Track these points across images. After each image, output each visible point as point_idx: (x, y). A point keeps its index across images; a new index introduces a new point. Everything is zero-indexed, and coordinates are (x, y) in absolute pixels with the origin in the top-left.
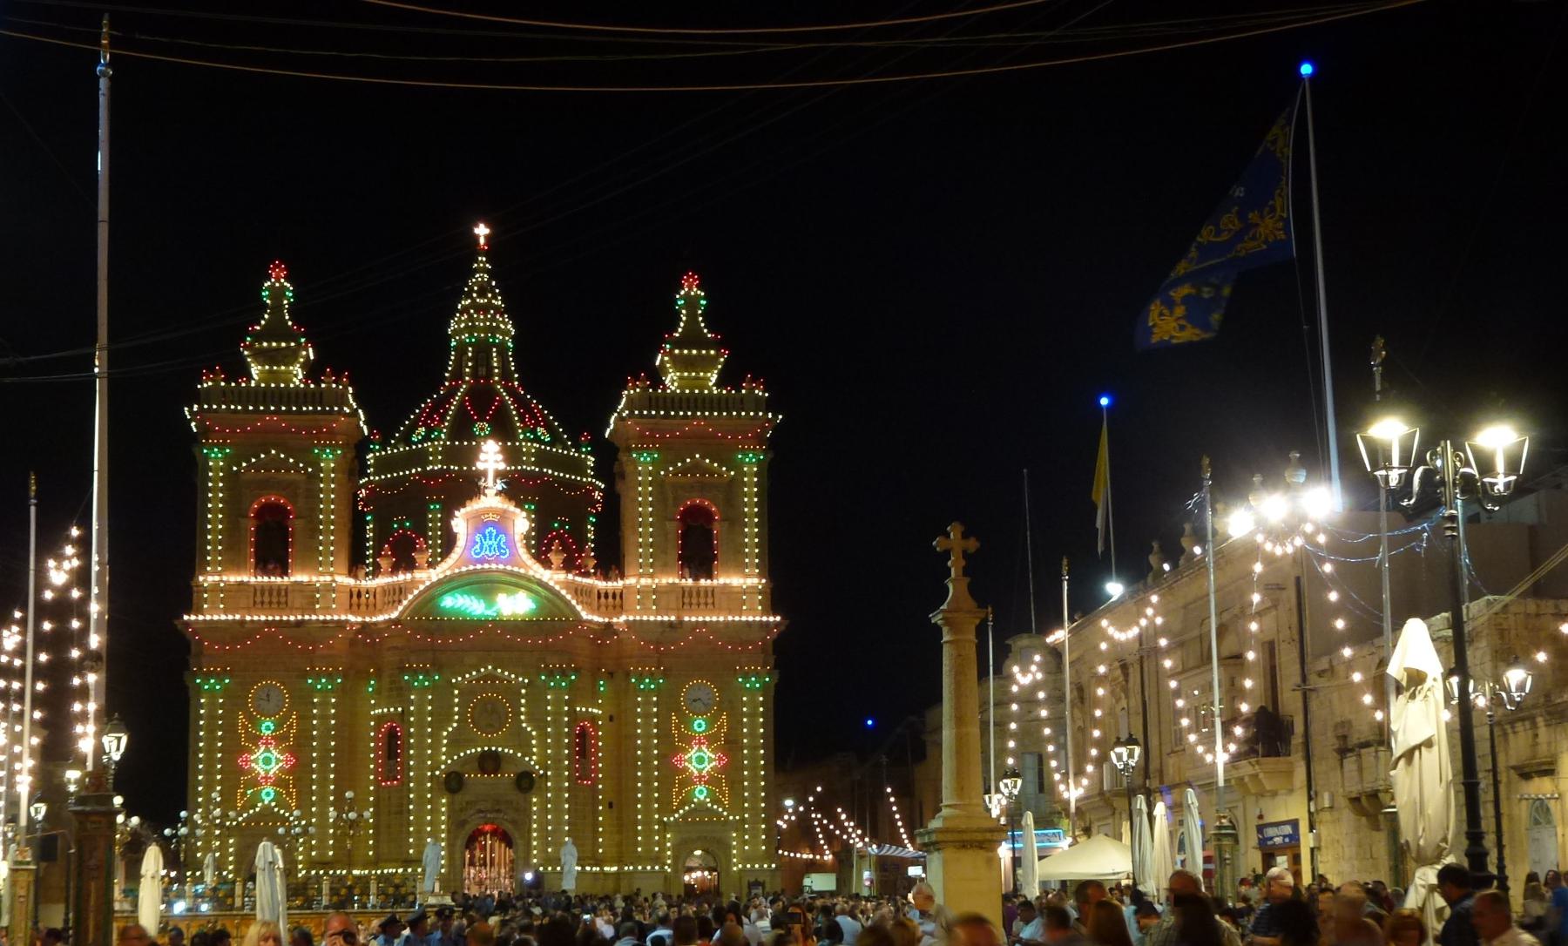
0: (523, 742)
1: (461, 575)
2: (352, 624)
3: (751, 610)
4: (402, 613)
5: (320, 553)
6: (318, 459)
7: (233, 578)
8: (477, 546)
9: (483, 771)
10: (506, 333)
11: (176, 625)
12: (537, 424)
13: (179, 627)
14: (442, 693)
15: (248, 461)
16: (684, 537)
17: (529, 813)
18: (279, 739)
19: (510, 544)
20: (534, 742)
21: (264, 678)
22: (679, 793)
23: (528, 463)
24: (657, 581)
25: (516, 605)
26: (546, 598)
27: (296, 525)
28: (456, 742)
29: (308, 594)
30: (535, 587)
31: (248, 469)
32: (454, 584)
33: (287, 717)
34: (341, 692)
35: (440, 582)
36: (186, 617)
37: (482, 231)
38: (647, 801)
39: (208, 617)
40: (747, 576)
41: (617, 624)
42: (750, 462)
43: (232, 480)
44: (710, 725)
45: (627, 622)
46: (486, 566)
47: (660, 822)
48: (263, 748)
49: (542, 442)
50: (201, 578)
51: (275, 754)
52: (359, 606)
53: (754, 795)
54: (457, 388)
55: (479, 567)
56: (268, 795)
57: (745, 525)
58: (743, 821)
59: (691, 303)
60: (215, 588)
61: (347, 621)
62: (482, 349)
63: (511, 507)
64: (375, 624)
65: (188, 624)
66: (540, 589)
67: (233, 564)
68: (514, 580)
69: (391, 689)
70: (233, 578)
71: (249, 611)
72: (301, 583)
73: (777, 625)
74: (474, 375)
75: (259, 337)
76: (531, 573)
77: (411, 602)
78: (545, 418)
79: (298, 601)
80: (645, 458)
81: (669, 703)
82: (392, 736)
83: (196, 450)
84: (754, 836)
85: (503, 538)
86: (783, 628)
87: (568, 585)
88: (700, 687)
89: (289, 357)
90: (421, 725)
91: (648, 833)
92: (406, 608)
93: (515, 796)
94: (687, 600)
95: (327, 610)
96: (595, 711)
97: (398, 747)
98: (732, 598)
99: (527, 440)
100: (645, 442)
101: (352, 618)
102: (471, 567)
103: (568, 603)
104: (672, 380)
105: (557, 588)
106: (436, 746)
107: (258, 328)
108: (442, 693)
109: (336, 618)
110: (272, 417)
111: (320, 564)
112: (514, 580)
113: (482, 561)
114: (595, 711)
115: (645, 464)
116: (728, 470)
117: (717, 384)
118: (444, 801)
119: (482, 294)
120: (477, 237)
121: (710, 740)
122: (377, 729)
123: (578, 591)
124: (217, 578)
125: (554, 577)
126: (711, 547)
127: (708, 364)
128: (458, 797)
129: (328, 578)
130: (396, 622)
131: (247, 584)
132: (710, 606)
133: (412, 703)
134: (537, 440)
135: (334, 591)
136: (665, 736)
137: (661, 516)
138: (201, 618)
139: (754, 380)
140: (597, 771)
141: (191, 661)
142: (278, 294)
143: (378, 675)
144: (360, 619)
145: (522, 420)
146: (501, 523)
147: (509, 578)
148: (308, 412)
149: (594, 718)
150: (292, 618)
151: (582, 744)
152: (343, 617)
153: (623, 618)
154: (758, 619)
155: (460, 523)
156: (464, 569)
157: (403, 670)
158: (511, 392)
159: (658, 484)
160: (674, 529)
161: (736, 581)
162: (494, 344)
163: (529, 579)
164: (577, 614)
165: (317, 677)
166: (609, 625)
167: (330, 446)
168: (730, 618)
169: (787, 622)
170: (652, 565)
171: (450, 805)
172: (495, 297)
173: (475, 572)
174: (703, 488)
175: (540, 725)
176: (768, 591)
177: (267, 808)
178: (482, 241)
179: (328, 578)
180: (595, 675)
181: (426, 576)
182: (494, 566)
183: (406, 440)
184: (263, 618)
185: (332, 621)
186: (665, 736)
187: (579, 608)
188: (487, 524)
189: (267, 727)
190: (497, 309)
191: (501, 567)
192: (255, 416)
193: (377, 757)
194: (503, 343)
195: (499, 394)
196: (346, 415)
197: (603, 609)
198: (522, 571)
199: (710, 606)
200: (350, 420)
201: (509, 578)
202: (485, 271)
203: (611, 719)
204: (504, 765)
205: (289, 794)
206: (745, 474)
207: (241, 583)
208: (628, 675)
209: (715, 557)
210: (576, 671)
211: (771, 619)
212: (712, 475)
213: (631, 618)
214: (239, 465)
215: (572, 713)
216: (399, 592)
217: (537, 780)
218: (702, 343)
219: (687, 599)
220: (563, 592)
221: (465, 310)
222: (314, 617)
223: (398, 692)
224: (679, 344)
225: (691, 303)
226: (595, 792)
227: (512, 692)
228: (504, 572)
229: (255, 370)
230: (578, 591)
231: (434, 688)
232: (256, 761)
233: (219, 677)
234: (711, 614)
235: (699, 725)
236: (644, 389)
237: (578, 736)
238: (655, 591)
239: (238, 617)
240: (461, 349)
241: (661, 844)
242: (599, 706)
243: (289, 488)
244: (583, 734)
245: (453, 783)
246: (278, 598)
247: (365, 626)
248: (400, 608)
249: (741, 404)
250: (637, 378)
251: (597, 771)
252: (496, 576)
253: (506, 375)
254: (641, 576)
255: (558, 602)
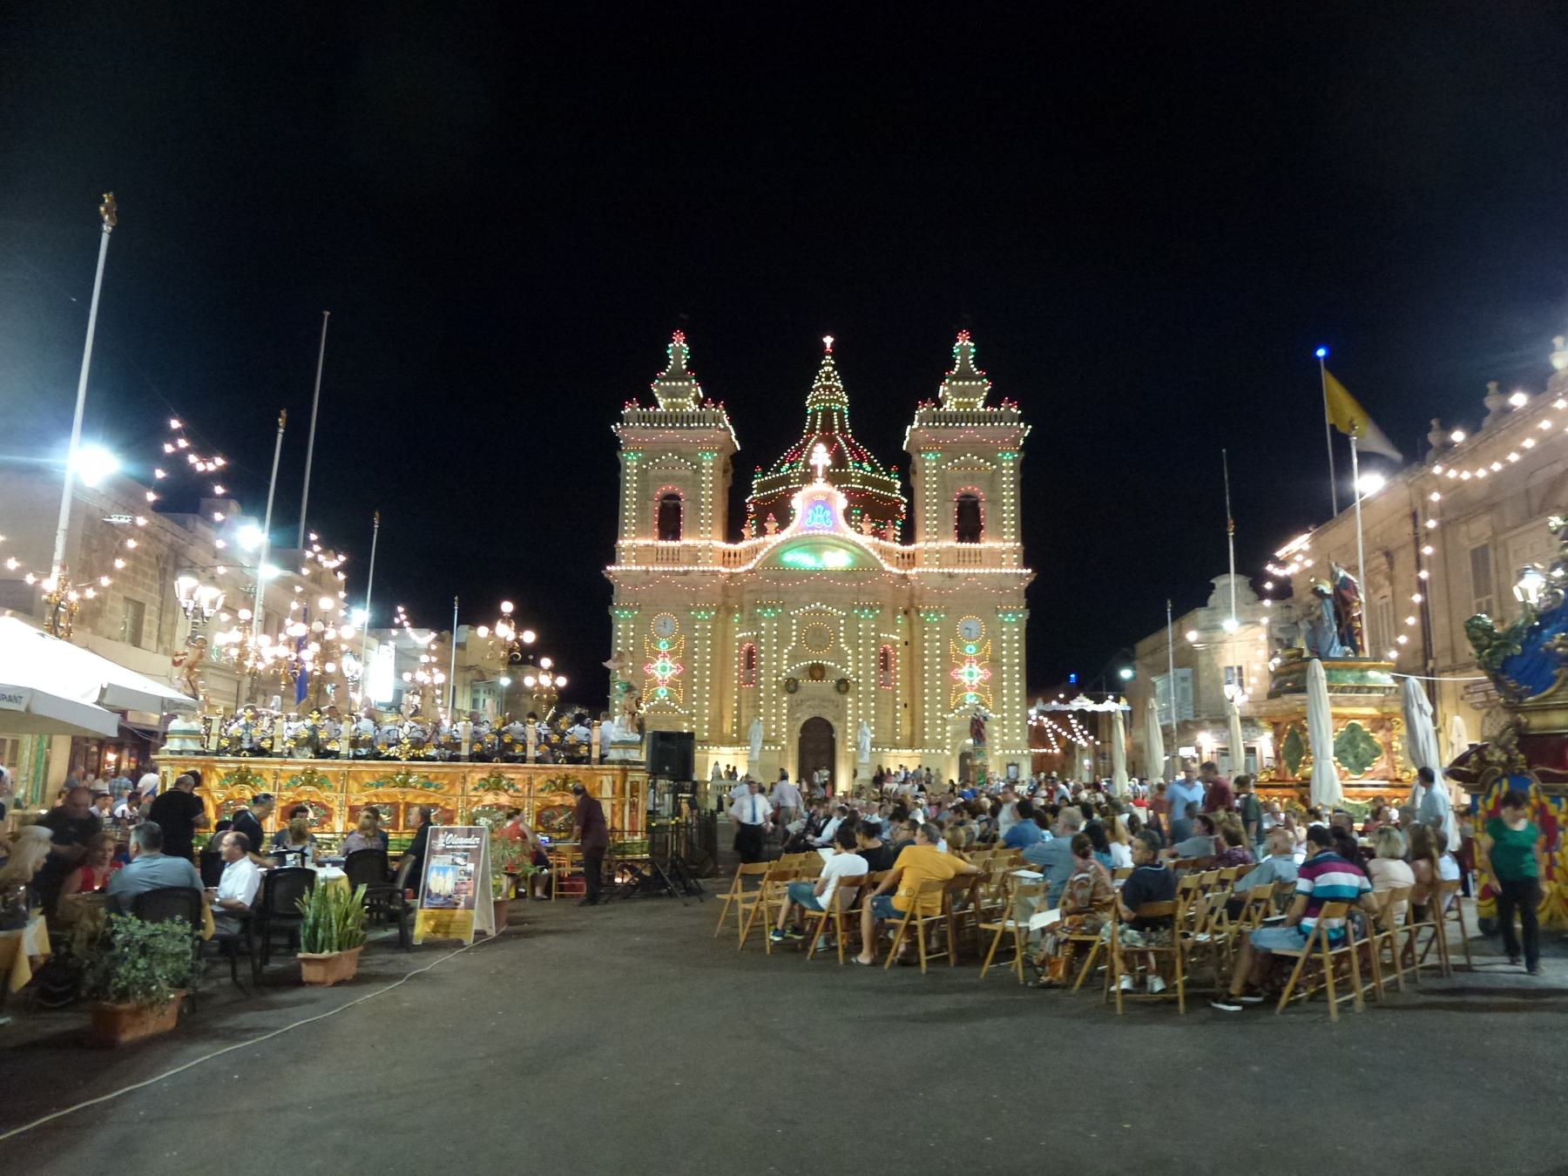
0: (841, 658)
1: (798, 538)
2: (722, 574)
3: (1009, 565)
4: (756, 565)
5: (702, 525)
6: (702, 460)
7: (642, 542)
8: (810, 518)
9: (813, 678)
10: (843, 403)
11: (603, 575)
12: (862, 461)
13: (606, 575)
14: (784, 621)
15: (654, 461)
16: (959, 513)
17: (845, 709)
18: (672, 654)
19: (833, 517)
20: (849, 658)
21: (662, 611)
22: (956, 697)
23: (855, 483)
24: (939, 544)
25: (838, 560)
26: (857, 555)
27: (685, 506)
28: (794, 658)
29: (694, 555)
30: (851, 547)
31: (652, 467)
32: (793, 545)
33: (676, 639)
34: (714, 621)
35: (783, 542)
36: (608, 568)
37: (828, 340)
38: (932, 703)
39: (624, 568)
40: (1005, 541)
41: (911, 575)
42: (1009, 461)
43: (643, 473)
44: (980, 646)
45: (918, 574)
46: (816, 532)
47: (942, 718)
48: (661, 659)
49: (864, 470)
50: (620, 542)
51: (669, 664)
52: (729, 562)
53: (1011, 700)
54: (812, 437)
55: (811, 532)
56: (662, 692)
57: (1004, 504)
58: (1003, 719)
59: (964, 351)
60: (630, 549)
61: (719, 571)
62: (828, 414)
63: (833, 490)
64: (738, 574)
65: (610, 573)
66: (854, 548)
67: (641, 533)
68: (836, 542)
69: (749, 620)
70: (642, 542)
71: (652, 564)
72: (688, 546)
73: (1028, 575)
74: (822, 430)
75: (664, 379)
76: (848, 536)
77: (763, 557)
78: (868, 457)
79: (684, 557)
80: (931, 456)
81: (949, 633)
82: (750, 653)
83: (619, 454)
84: (1012, 729)
85: (828, 513)
86: (1032, 579)
87: (875, 546)
88: (973, 622)
89: (683, 393)
90: (769, 645)
91: (933, 726)
92: (759, 561)
93: (835, 696)
94: (961, 559)
95: (706, 563)
96: (895, 637)
97: (753, 660)
98: (996, 558)
99: (855, 468)
100: (933, 445)
101: (723, 569)
102: (805, 533)
103: (874, 558)
104: (950, 406)
105: (867, 547)
106: (778, 660)
107: (664, 374)
108: (784, 621)
109: (711, 568)
110: (670, 433)
111: (702, 532)
112: (836, 542)
113: (813, 528)
114: (895, 637)
115: (931, 461)
116: (992, 465)
117: (985, 406)
118: (785, 699)
119: (828, 378)
120: (824, 344)
121: (980, 659)
122: (740, 648)
123: (882, 551)
124: (631, 542)
125: (867, 541)
126: (978, 520)
127: (976, 392)
128: (796, 696)
129: (707, 542)
130: (751, 571)
131: (653, 546)
132: (978, 563)
133: (762, 628)
134: (861, 467)
135: (711, 551)
136: (945, 656)
137: (943, 501)
138: (618, 568)
139: (1010, 401)
140: (896, 680)
141: (614, 599)
142: (678, 352)
143: (741, 611)
144: (728, 570)
145: (852, 455)
146: (827, 503)
147: (832, 541)
148: (694, 428)
149: (894, 643)
150: (681, 569)
151: (885, 661)
152: (716, 568)
153: (914, 571)
154: (1014, 571)
155: (798, 502)
156: (800, 534)
157: (756, 606)
158: (847, 442)
159: (941, 475)
160: (953, 508)
161: (997, 545)
162: (835, 410)
163: (846, 541)
164: (880, 566)
165: (699, 610)
166: (904, 577)
167: (709, 450)
168: (993, 570)
169: (1035, 574)
170: (935, 533)
171: (790, 703)
172: (836, 380)
173: (808, 536)
174: (972, 478)
175: (855, 646)
176: (1021, 552)
177: (661, 701)
178: (828, 346)
179: (707, 542)
180: (895, 612)
181: (773, 539)
182: (821, 532)
183: (778, 470)
184: (661, 569)
185: (708, 571)
186: (945, 656)
187: (882, 561)
188: (817, 503)
189: (663, 646)
190: (838, 388)
191: (826, 532)
192: (659, 431)
193: (740, 667)
194: (842, 409)
195: (837, 441)
196: (720, 429)
197: (901, 565)
198: (841, 535)
199: (978, 563)
200: (723, 433)
201: (832, 541)
202: (831, 365)
203: (906, 643)
204: (827, 674)
205: (678, 692)
206: (1003, 468)
207: (648, 546)
208: (918, 612)
209: (982, 528)
210: (881, 607)
211: (1024, 571)
212: (979, 469)
213: (920, 570)
214: (647, 465)
215: (877, 638)
216: (756, 550)
217: (851, 685)
218: (971, 377)
219: (961, 558)
220: (871, 550)
221: (817, 389)
222: (696, 568)
223: (753, 622)
224: (956, 378)
225: (964, 351)
226: (895, 695)
227: (834, 621)
228: (830, 536)
229: (661, 403)
230: (882, 551)
231: (778, 618)
232: (656, 669)
233: (631, 609)
234: (979, 567)
235: (971, 649)
236: (930, 409)
237: (882, 655)
238: (937, 552)
239: (644, 568)
240: (815, 413)
241: (944, 732)
242: (897, 634)
243: (683, 479)
244: (885, 654)
245: (791, 686)
246: (673, 557)
247: (732, 576)
248: (755, 561)
249: (998, 418)
250: (924, 401)
251: (896, 680)
252: (822, 540)
253: (842, 430)
254: (928, 541)
255: (867, 557)
